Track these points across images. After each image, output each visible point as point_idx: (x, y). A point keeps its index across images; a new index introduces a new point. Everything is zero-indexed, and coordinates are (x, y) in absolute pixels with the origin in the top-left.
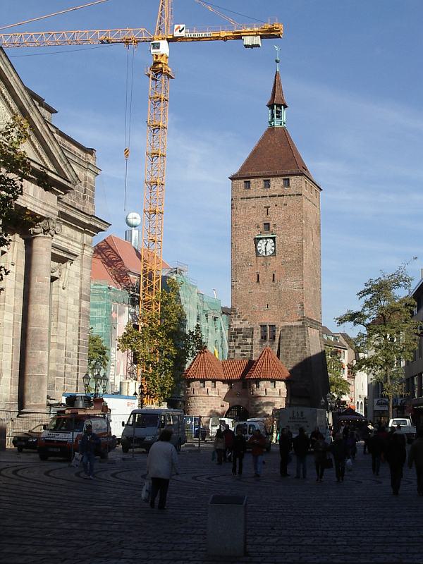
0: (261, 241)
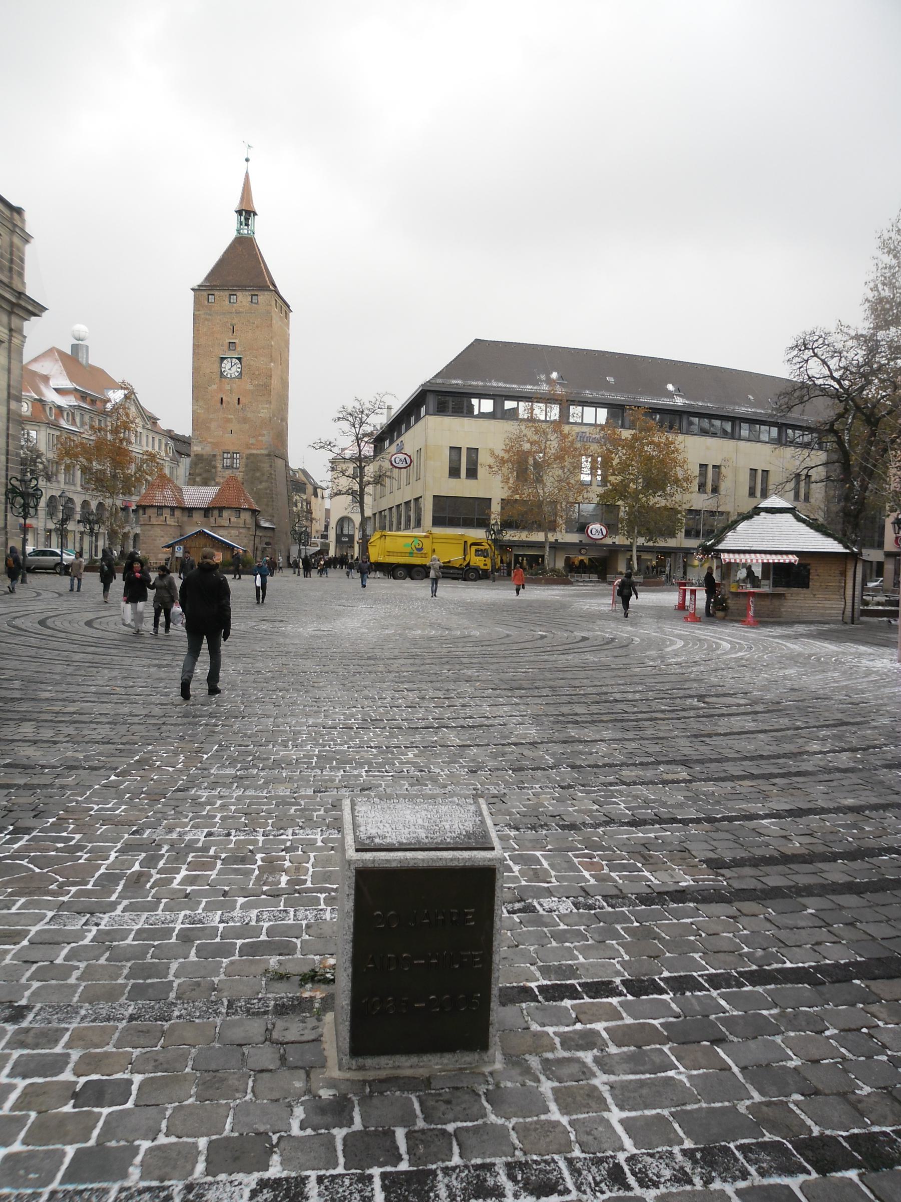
0: (225, 361)
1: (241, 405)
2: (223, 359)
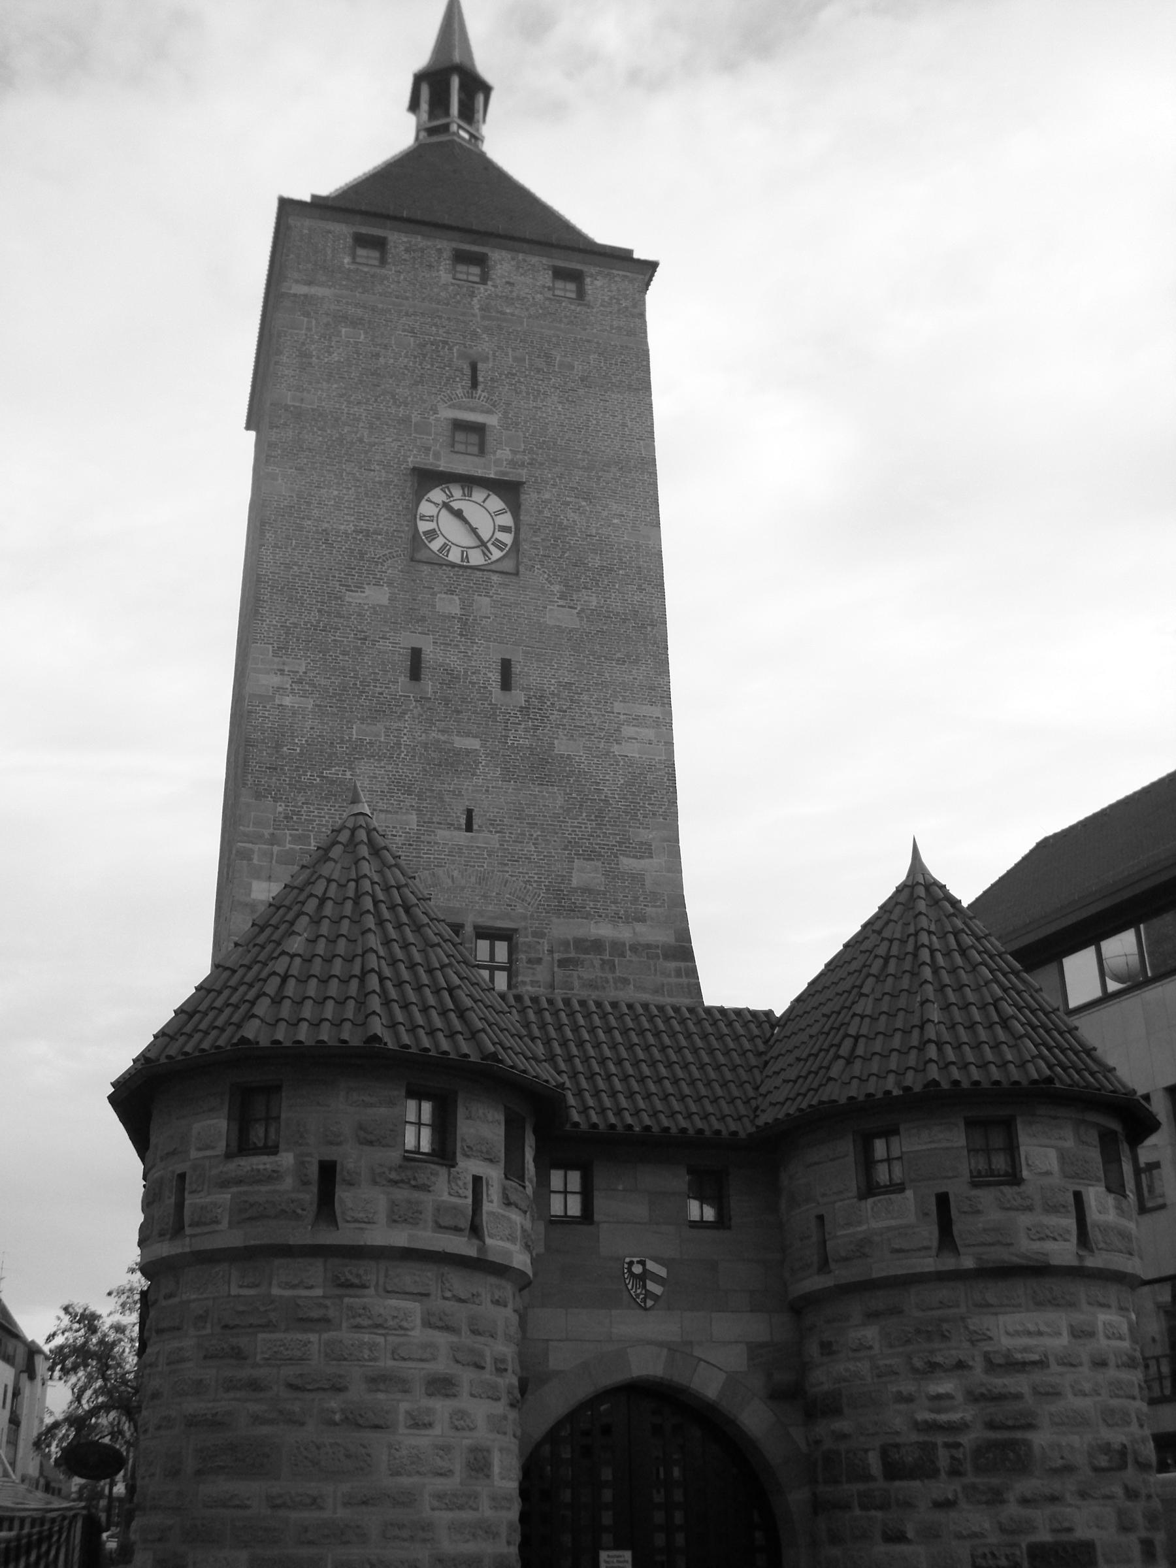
0: (437, 495)
1: (518, 697)
2: (428, 478)
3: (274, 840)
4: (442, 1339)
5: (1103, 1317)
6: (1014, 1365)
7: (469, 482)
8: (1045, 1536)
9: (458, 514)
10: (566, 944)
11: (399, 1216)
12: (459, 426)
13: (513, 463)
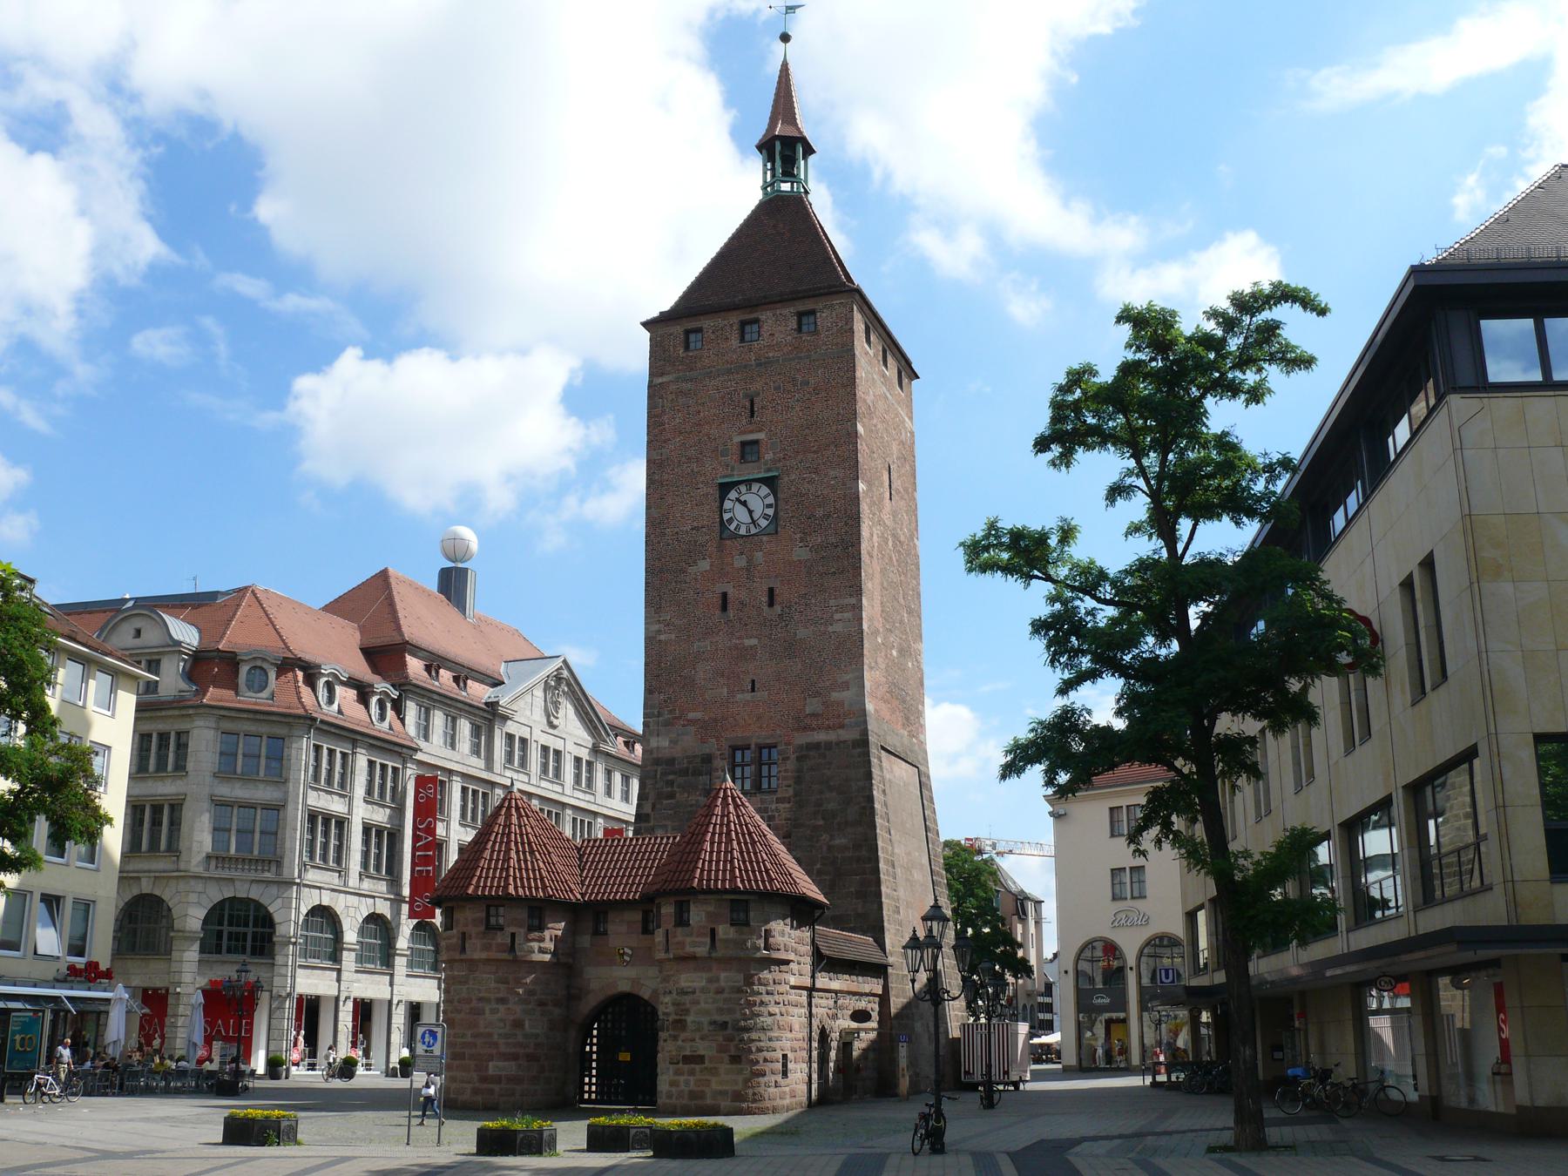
0: (733, 495)
1: (778, 609)
2: (725, 489)
3: (659, 715)
4: (502, 986)
5: (723, 975)
6: (683, 992)
7: (748, 483)
8: (688, 1053)
9: (744, 504)
10: (801, 747)
11: (486, 948)
12: (743, 444)
13: (774, 461)
